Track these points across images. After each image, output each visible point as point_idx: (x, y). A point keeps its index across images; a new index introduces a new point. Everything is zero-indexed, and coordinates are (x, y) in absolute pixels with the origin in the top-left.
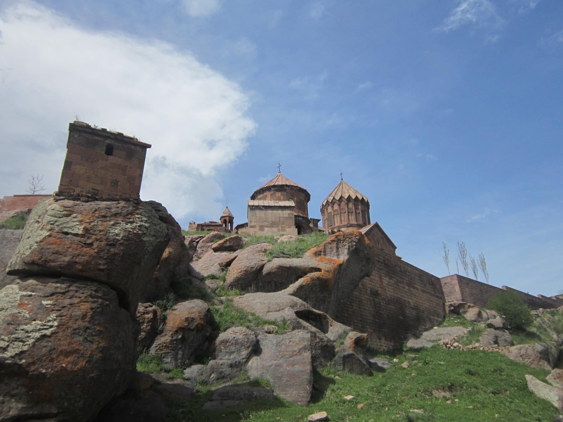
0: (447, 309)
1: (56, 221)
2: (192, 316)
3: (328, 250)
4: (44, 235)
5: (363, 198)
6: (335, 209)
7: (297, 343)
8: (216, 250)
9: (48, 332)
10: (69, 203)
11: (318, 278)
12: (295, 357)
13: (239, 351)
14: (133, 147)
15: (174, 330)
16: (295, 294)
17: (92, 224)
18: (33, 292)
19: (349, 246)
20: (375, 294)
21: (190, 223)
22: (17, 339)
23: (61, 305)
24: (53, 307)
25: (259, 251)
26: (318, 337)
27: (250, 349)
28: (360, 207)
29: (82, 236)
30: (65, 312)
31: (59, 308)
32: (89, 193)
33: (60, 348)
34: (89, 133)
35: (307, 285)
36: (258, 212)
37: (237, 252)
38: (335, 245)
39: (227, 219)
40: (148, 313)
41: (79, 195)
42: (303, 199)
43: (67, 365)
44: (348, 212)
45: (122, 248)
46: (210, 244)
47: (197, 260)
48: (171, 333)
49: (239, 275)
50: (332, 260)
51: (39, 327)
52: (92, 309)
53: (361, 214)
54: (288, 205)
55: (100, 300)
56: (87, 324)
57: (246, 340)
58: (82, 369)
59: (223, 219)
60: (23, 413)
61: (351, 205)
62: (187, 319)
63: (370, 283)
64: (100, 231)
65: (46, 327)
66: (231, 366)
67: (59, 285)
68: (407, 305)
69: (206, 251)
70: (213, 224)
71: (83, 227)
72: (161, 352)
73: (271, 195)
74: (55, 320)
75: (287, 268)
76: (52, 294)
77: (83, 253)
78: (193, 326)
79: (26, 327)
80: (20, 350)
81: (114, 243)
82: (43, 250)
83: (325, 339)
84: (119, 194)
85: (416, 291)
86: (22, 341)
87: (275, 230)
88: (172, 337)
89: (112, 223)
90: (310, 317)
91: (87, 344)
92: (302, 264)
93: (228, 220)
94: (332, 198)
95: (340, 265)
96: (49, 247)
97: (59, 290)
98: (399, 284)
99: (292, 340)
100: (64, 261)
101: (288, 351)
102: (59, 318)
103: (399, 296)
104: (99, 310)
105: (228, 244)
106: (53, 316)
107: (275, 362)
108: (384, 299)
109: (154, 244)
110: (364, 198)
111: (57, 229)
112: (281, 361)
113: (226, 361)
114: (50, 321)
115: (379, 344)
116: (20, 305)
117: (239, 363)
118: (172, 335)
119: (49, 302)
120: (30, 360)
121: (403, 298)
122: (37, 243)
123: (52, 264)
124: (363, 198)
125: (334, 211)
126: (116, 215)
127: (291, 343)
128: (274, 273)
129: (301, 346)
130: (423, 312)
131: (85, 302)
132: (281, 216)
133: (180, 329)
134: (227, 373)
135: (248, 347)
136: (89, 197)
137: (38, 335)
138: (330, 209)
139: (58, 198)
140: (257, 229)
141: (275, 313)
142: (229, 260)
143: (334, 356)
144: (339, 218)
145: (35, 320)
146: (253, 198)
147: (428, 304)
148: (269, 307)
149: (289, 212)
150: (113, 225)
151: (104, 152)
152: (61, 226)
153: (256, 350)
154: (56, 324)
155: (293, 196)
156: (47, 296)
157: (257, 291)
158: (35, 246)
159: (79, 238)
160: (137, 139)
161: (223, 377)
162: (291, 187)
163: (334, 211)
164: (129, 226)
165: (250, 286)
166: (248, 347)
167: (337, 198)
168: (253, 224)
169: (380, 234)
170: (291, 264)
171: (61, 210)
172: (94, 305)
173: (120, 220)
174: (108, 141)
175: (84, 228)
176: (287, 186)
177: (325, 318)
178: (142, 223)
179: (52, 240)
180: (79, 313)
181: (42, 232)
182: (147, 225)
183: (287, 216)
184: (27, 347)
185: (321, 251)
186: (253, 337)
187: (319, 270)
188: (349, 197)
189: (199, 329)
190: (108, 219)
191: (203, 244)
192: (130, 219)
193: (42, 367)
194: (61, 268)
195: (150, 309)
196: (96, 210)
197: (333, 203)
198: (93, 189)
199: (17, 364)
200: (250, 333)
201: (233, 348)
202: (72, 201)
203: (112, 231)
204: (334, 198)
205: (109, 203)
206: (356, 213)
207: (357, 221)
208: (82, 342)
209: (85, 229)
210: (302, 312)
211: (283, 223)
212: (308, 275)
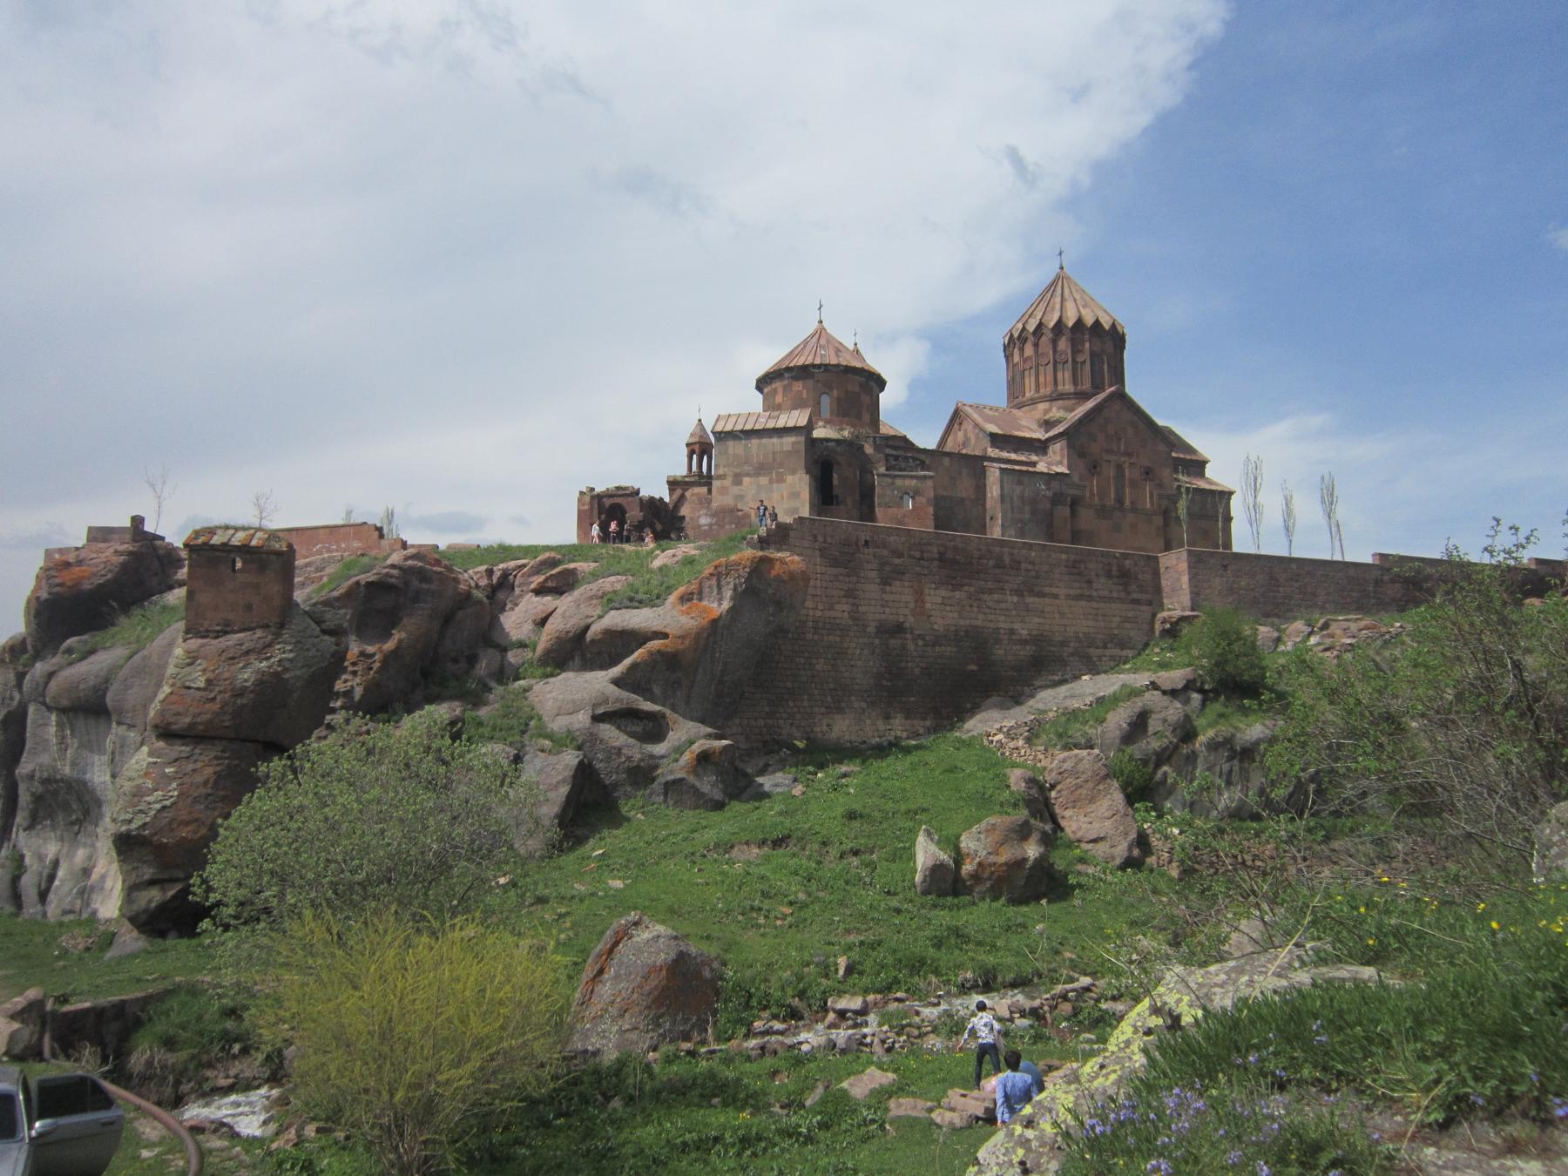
0: (1158, 627)
3: (706, 590)
8: (540, 591)
9: (168, 803)
10: (195, 643)
16: (617, 682)
22: (141, 811)
25: (591, 598)
28: (1087, 345)
29: (204, 689)
30: (186, 779)
36: (731, 443)
38: (714, 582)
42: (857, 389)
44: (1055, 362)
49: (548, 645)
61: (1063, 344)
73: (785, 388)
87: (764, 480)
94: (1020, 326)
95: (714, 622)
103: (979, 623)
105: (550, 584)
106: (174, 785)
108: (921, 637)
110: (1102, 321)
116: (147, 774)
125: (1025, 361)
126: (247, 653)
130: (1063, 644)
132: (778, 449)
137: (158, 806)
140: (728, 482)
143: (653, 780)
147: (1090, 623)
149: (793, 439)
155: (830, 388)
159: (203, 693)
162: (826, 368)
164: (264, 664)
165: (572, 658)
167: (1031, 327)
173: (252, 657)
176: (814, 366)
177: (663, 716)
179: (174, 698)
187: (665, 636)
197: (1022, 338)
204: (1024, 329)
206: (1074, 362)
207: (1075, 382)
209: (209, 681)
211: (781, 465)
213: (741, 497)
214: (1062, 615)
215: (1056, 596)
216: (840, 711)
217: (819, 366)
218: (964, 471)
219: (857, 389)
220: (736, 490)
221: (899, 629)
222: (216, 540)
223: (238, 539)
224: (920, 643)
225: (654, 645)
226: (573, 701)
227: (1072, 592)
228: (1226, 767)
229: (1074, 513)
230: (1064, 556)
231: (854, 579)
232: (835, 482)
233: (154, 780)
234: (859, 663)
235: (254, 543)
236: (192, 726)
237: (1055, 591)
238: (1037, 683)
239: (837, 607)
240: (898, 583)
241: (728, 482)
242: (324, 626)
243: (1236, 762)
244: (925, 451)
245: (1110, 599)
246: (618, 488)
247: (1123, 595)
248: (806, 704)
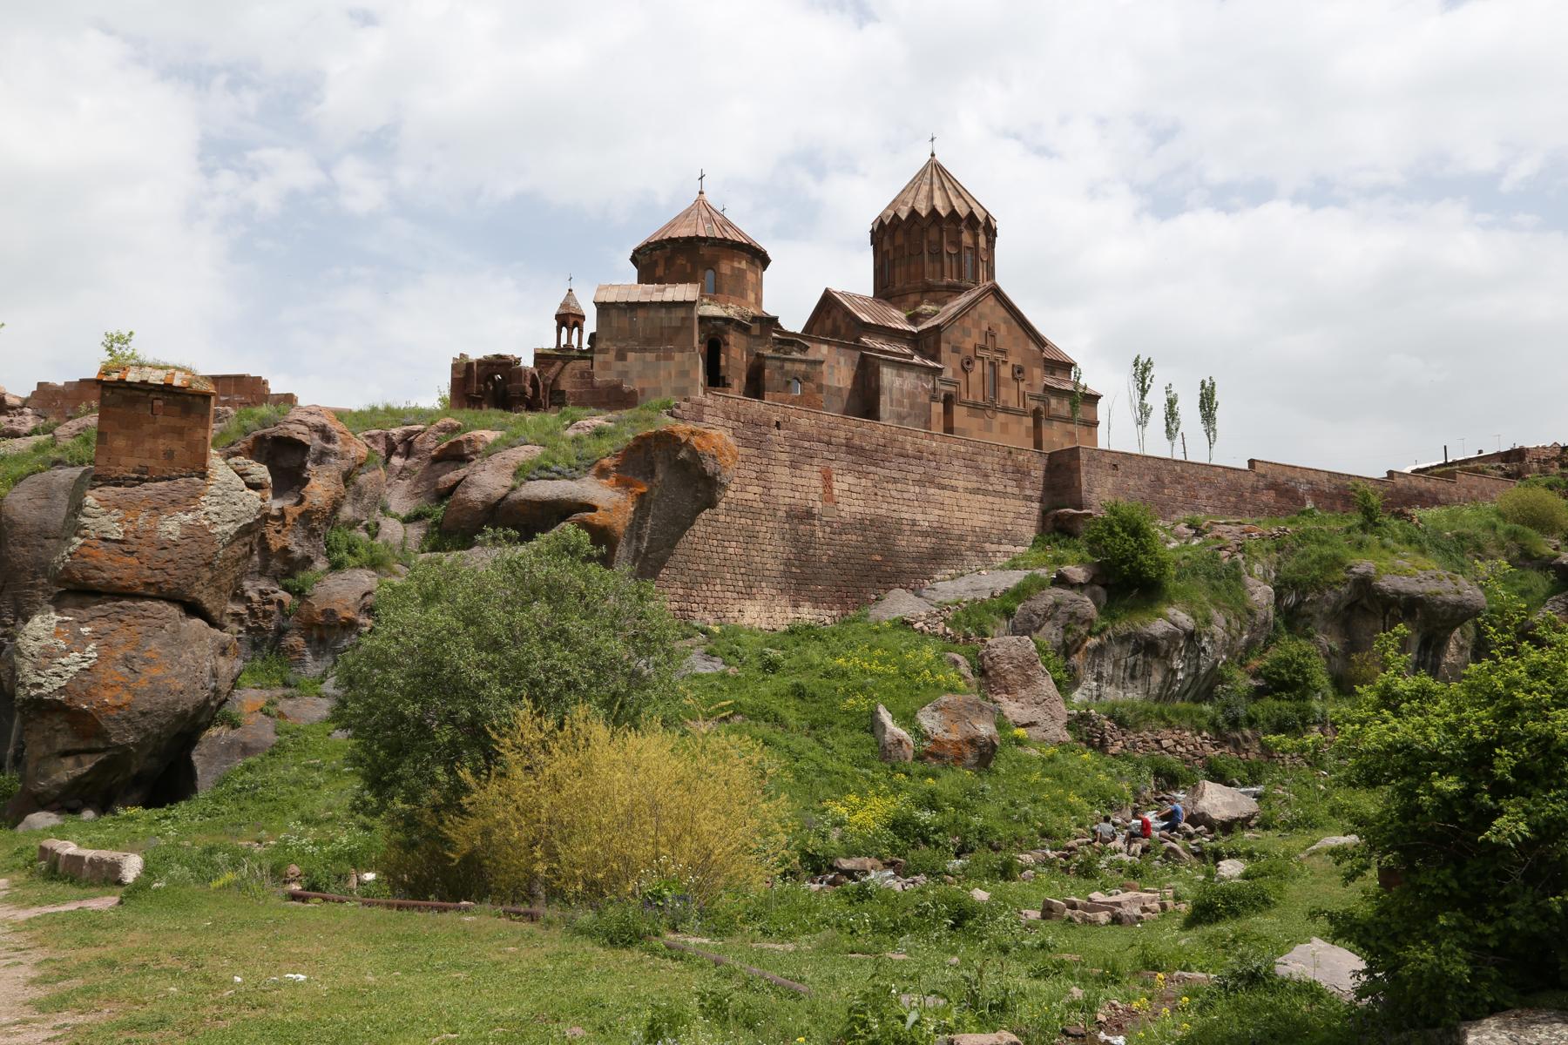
5: (971, 215)
9: (85, 665)
62: (324, 612)
87: (650, 356)
94: (892, 213)
103: (883, 512)
116: (57, 634)
121: (895, 515)
130: (961, 538)
137: (76, 669)
140: (611, 356)
147: (987, 518)
167: (903, 216)
169: (1002, 312)
182: (217, 509)
187: (593, 508)
211: (670, 341)
213: (624, 374)
214: (960, 508)
215: (954, 489)
216: (751, 597)
217: (705, 239)
218: (842, 360)
220: (619, 365)
221: (809, 515)
222: (132, 376)
223: (156, 377)
224: (828, 529)
227: (970, 485)
228: (1131, 660)
229: (948, 411)
230: (963, 449)
231: (765, 461)
232: (723, 363)
234: (769, 548)
235: (177, 382)
237: (954, 483)
238: (938, 577)
239: (749, 488)
240: (807, 467)
242: (248, 479)
243: (1140, 656)
244: (794, 334)
245: (1004, 495)
247: (1016, 491)
248: (718, 588)
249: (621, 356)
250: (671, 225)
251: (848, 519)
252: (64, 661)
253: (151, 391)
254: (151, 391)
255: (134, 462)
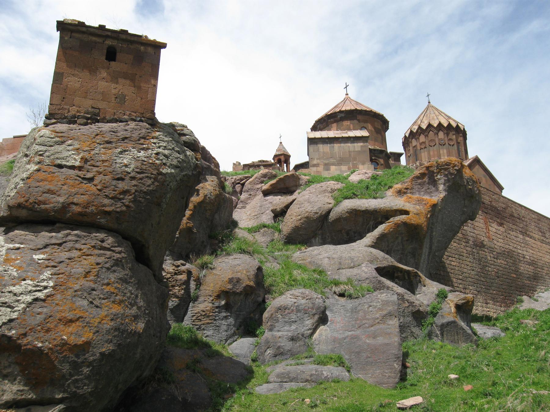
1: (46, 151)
2: (239, 275)
4: (32, 169)
5: (457, 126)
6: (421, 141)
7: (379, 309)
8: (266, 193)
10: (62, 127)
11: (405, 224)
12: (377, 327)
13: (302, 319)
14: (142, 48)
15: (216, 294)
17: (93, 152)
18: (22, 244)
19: (445, 180)
20: (480, 245)
21: (234, 164)
23: (57, 260)
24: (46, 262)
25: (325, 191)
26: (407, 300)
27: (317, 317)
29: (80, 168)
30: (62, 268)
31: (55, 264)
32: (88, 114)
33: (58, 316)
34: (83, 33)
35: (390, 233)
36: (321, 146)
37: (296, 193)
38: (426, 179)
39: (282, 158)
40: (180, 273)
41: (74, 116)
42: (380, 127)
43: (68, 337)
45: (134, 182)
46: (259, 186)
47: (244, 207)
48: (211, 299)
49: (298, 224)
50: (423, 200)
51: (30, 288)
52: (98, 264)
53: (455, 146)
54: (360, 135)
55: (108, 253)
56: (93, 285)
57: (311, 305)
58: (88, 344)
59: (276, 159)
60: (20, 397)
61: (441, 135)
62: (231, 281)
63: (472, 230)
64: (103, 161)
65: (38, 288)
66: (292, 339)
67: (54, 234)
68: (522, 259)
69: (255, 195)
70: (263, 163)
71: (80, 156)
72: (199, 323)
74: (50, 279)
75: (363, 211)
76: (46, 246)
77: (81, 191)
78: (239, 288)
79: (14, 288)
80: (8, 318)
81: (123, 176)
82: (31, 189)
83: (417, 303)
84: (128, 113)
85: (533, 241)
86: (9, 307)
87: (344, 168)
88: (213, 304)
89: (119, 150)
90: (396, 275)
91: (94, 311)
92: (382, 206)
93: (283, 158)
95: (434, 206)
96: (38, 184)
97: (54, 241)
98: (512, 233)
99: (372, 304)
100: (58, 202)
101: (368, 319)
102: (56, 276)
103: (511, 248)
104: (107, 265)
107: (350, 333)
109: (178, 179)
110: (460, 125)
111: (47, 161)
112: (358, 332)
113: (286, 333)
114: (44, 280)
115: (485, 309)
116: (7, 261)
117: (303, 335)
118: (213, 300)
119: (42, 256)
120: (22, 331)
121: (516, 250)
122: (23, 180)
123: (43, 206)
124: (457, 126)
125: (421, 144)
127: (371, 309)
128: (346, 219)
129: (385, 312)
131: (88, 255)
132: (352, 149)
133: (223, 294)
134: (287, 348)
135: (314, 315)
136: (88, 119)
137: (29, 298)
138: (414, 142)
139: (48, 121)
140: (321, 168)
141: (348, 270)
142: (285, 205)
144: (426, 153)
145: (24, 280)
146: (314, 128)
148: (340, 263)
149: (362, 144)
150: (121, 153)
151: (104, 57)
152: (52, 157)
153: (323, 320)
154: (51, 284)
156: (39, 249)
157: (324, 243)
158: (21, 184)
159: (77, 172)
160: (146, 37)
161: (282, 354)
163: (421, 144)
164: (142, 153)
166: (314, 315)
167: (424, 127)
168: (315, 162)
170: (367, 205)
171: (52, 136)
172: (101, 260)
173: (130, 146)
174: (109, 42)
175: (82, 158)
177: (416, 275)
178: (160, 150)
179: (42, 175)
180: (80, 270)
181: (28, 166)
182: (166, 152)
183: (360, 149)
184: (16, 314)
185: (407, 189)
186: (321, 301)
187: (406, 213)
188: (440, 124)
189: (248, 291)
190: (114, 145)
191: (249, 186)
192: (143, 144)
193: (37, 339)
194: (55, 212)
195: (183, 268)
196: (97, 135)
198: (93, 108)
199: (6, 336)
200: (315, 296)
201: (294, 317)
202: (67, 125)
203: (119, 161)
204: (420, 127)
205: (114, 125)
208: (86, 307)
209: (85, 160)
210: (384, 268)
211: (355, 159)
212: (391, 219)
219: (380, 127)
224: (492, 255)
225: (403, 217)
226: (352, 259)
230: (533, 216)
233: (19, 268)
236: (65, 207)
241: (321, 168)
246: (260, 161)
249: (328, 170)
250: (336, 107)
251: (499, 251)
252: (12, 288)
253: (107, 37)
254: (107, 37)
255: (87, 104)
